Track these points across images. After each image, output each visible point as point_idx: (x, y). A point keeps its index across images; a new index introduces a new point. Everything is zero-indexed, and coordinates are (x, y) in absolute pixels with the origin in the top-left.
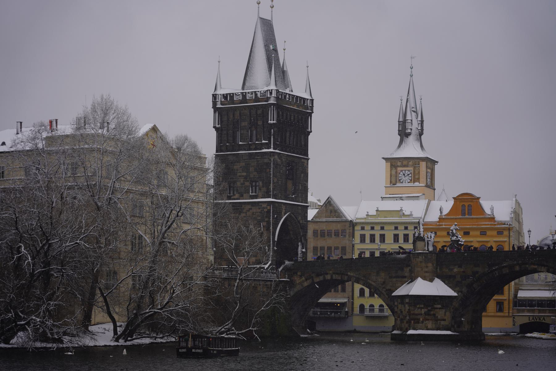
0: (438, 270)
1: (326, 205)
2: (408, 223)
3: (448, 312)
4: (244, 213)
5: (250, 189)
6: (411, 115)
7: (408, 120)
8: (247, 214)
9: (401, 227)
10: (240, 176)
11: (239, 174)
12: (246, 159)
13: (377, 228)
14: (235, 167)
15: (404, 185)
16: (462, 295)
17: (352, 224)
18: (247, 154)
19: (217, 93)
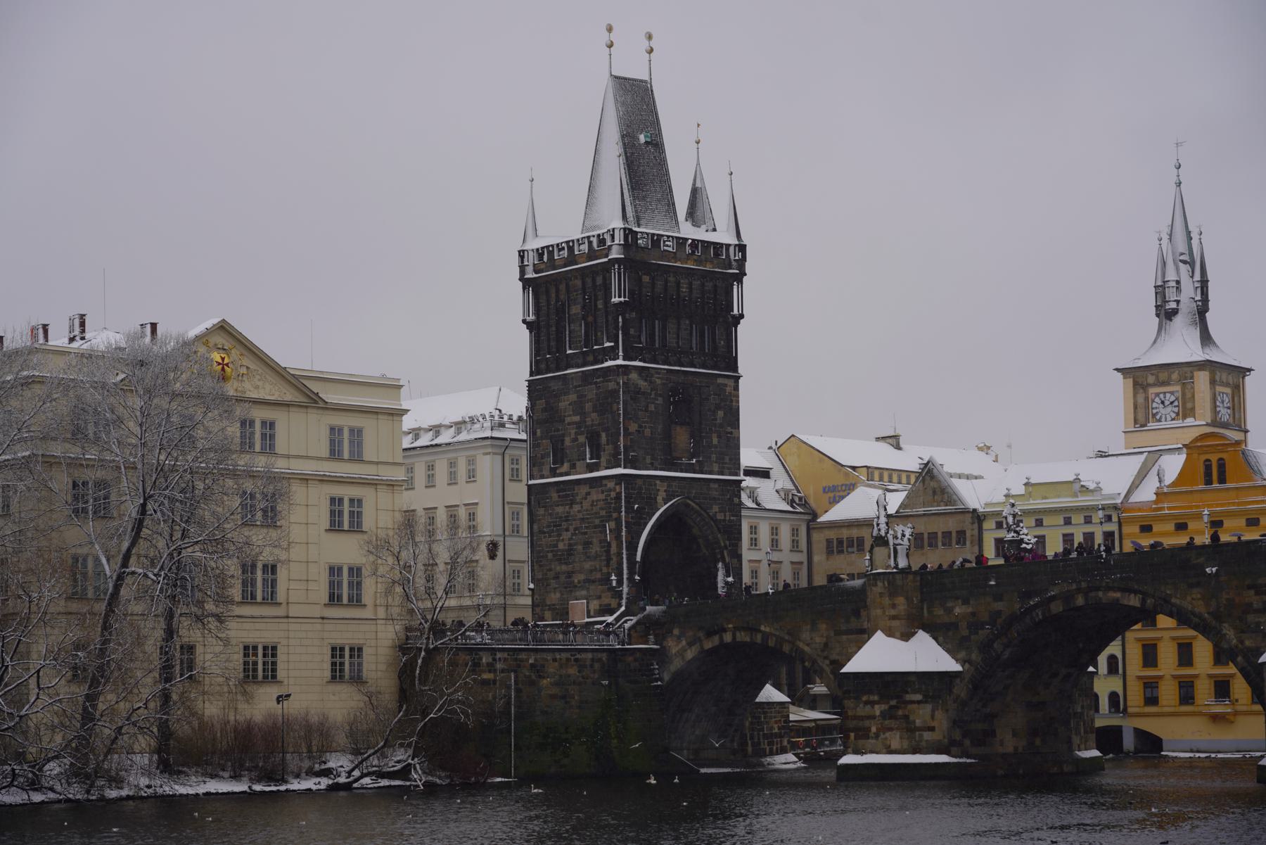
1: (923, 477)
2: (1090, 507)
3: (940, 711)
4: (577, 503)
5: (587, 450)
6: (1177, 269)
7: (1169, 281)
8: (584, 505)
9: (1078, 519)
10: (569, 424)
11: (568, 420)
12: (579, 386)
14: (562, 405)
15: (1163, 424)
16: (973, 669)
17: (978, 518)
18: (580, 374)
19: (525, 249)
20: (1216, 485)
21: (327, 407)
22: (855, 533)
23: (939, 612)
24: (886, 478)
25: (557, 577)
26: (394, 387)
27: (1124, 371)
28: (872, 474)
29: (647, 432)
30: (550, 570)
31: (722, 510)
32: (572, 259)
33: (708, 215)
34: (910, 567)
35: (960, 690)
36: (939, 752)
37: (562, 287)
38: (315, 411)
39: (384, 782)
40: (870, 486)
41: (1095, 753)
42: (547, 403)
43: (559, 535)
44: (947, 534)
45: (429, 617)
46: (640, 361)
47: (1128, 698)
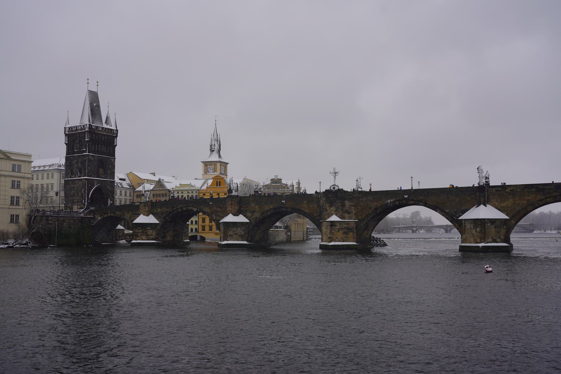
0: (152, 210)
11: (74, 166)
15: (210, 173)
17: (169, 191)
20: (218, 186)
21: (12, 160)
23: (155, 210)
24: (151, 182)
25: (70, 201)
26: (30, 156)
29: (93, 169)
30: (69, 199)
32: (77, 130)
33: (110, 123)
34: (149, 201)
35: (159, 227)
39: (22, 246)
40: (147, 183)
41: (188, 241)
44: (163, 194)
45: (35, 209)
46: (92, 153)
47: (199, 229)
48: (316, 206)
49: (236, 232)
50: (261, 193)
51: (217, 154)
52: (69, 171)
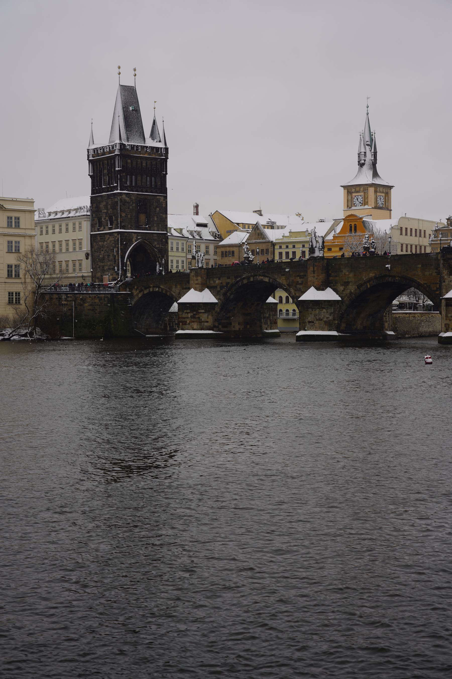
11: (103, 211)
13: (290, 246)
15: (357, 208)
17: (273, 244)
19: (89, 148)
22: (231, 249)
23: (212, 282)
25: (99, 267)
26: (31, 202)
27: (344, 187)
28: (245, 226)
29: (129, 216)
30: (98, 265)
31: (158, 244)
32: (104, 153)
35: (217, 309)
36: (209, 330)
37: (101, 163)
38: (2, 211)
42: (97, 205)
43: (100, 252)
44: (262, 250)
48: (434, 274)
49: (320, 317)
50: (373, 250)
51: (369, 171)
52: (96, 219)
